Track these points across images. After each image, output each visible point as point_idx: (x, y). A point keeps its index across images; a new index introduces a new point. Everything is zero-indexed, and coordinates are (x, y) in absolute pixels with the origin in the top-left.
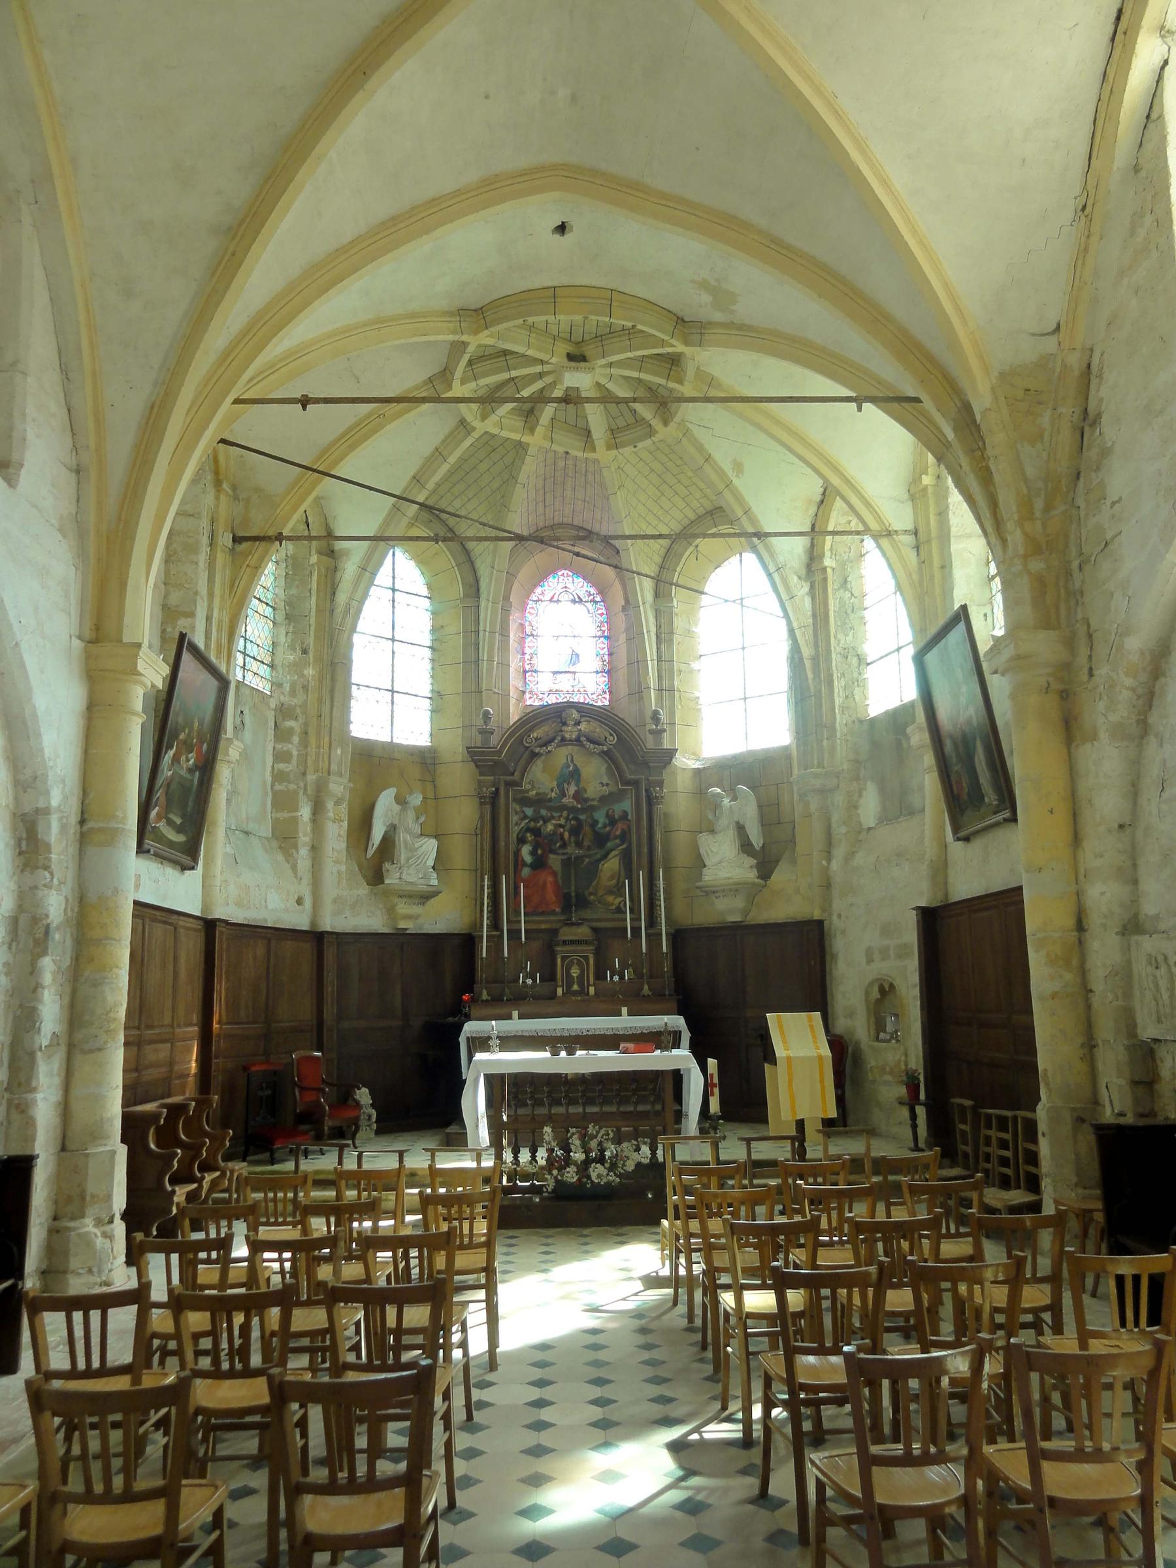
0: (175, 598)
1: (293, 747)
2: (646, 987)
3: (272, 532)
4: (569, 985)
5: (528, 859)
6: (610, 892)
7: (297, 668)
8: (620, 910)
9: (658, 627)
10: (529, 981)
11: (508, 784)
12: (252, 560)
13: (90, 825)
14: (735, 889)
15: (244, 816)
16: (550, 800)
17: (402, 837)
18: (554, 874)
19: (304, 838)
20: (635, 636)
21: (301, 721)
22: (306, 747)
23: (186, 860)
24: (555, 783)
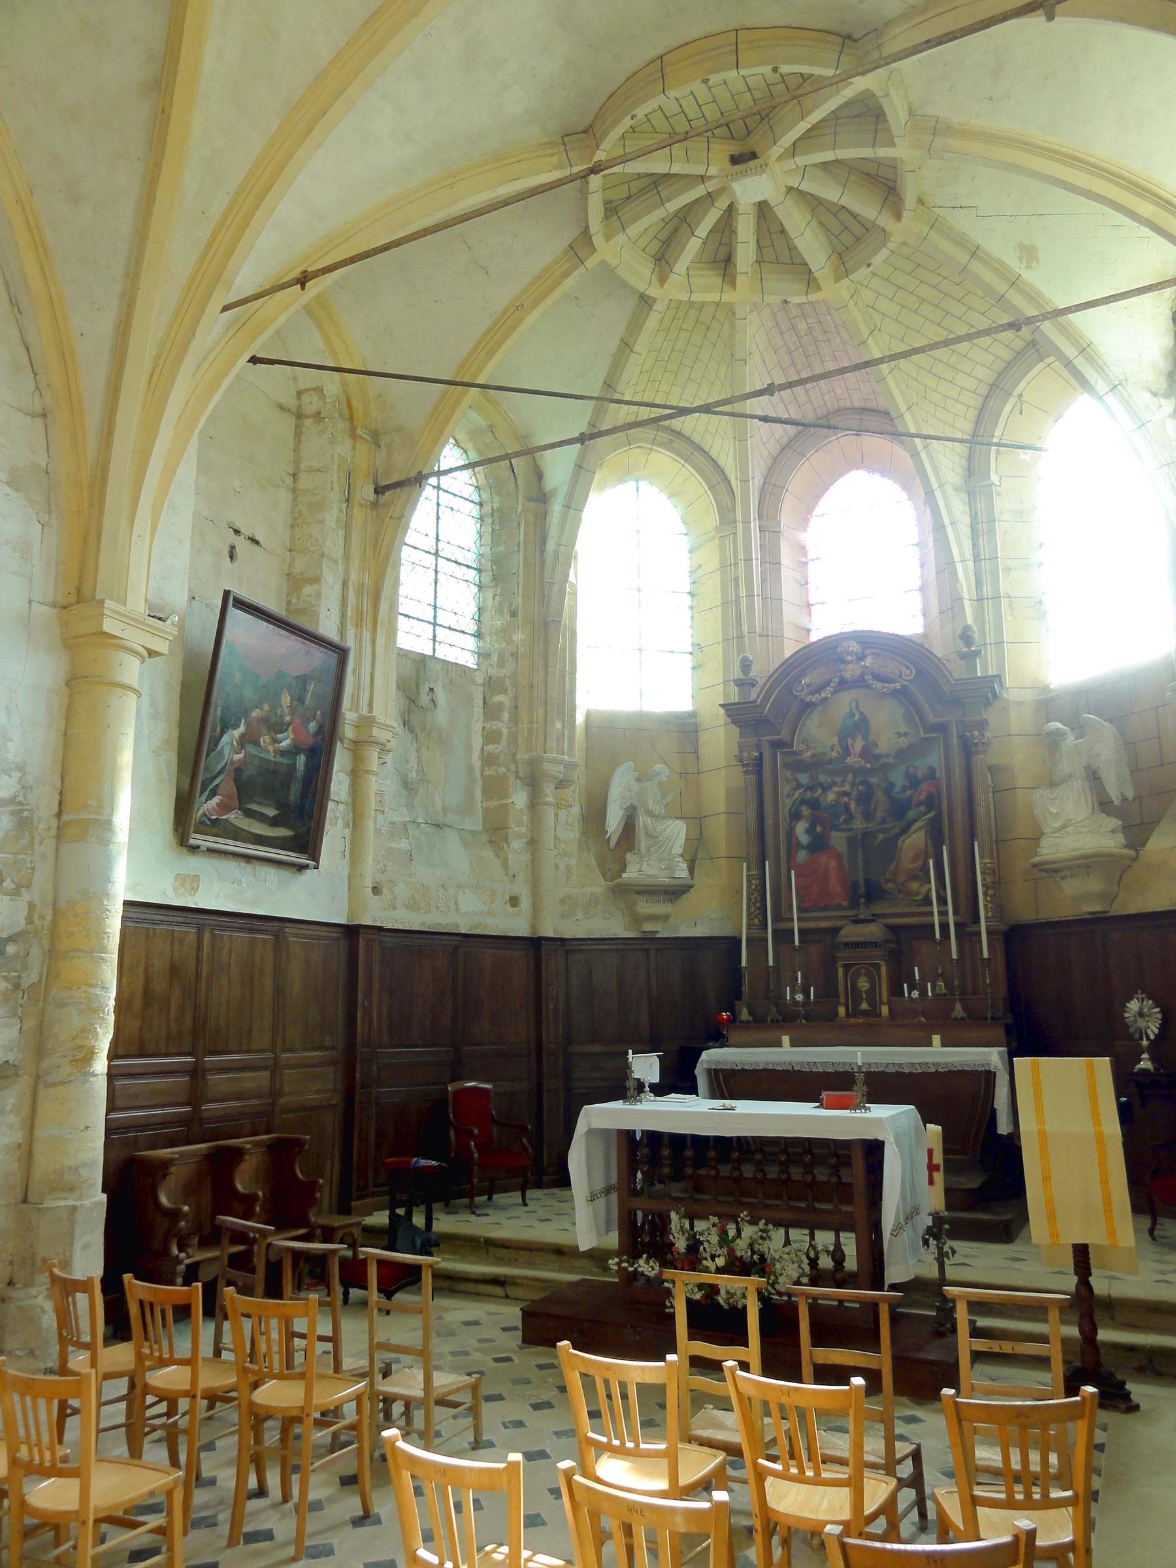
0: (299, 566)
1: (502, 726)
2: (958, 1006)
3: (413, 474)
4: (857, 1001)
5: (804, 839)
6: (915, 878)
7: (504, 633)
8: (927, 901)
9: (974, 516)
10: (799, 997)
11: (776, 745)
14: (1087, 864)
15: (439, 806)
16: (830, 761)
17: (642, 820)
18: (839, 857)
19: (518, 829)
21: (511, 693)
22: (516, 723)
24: (835, 740)
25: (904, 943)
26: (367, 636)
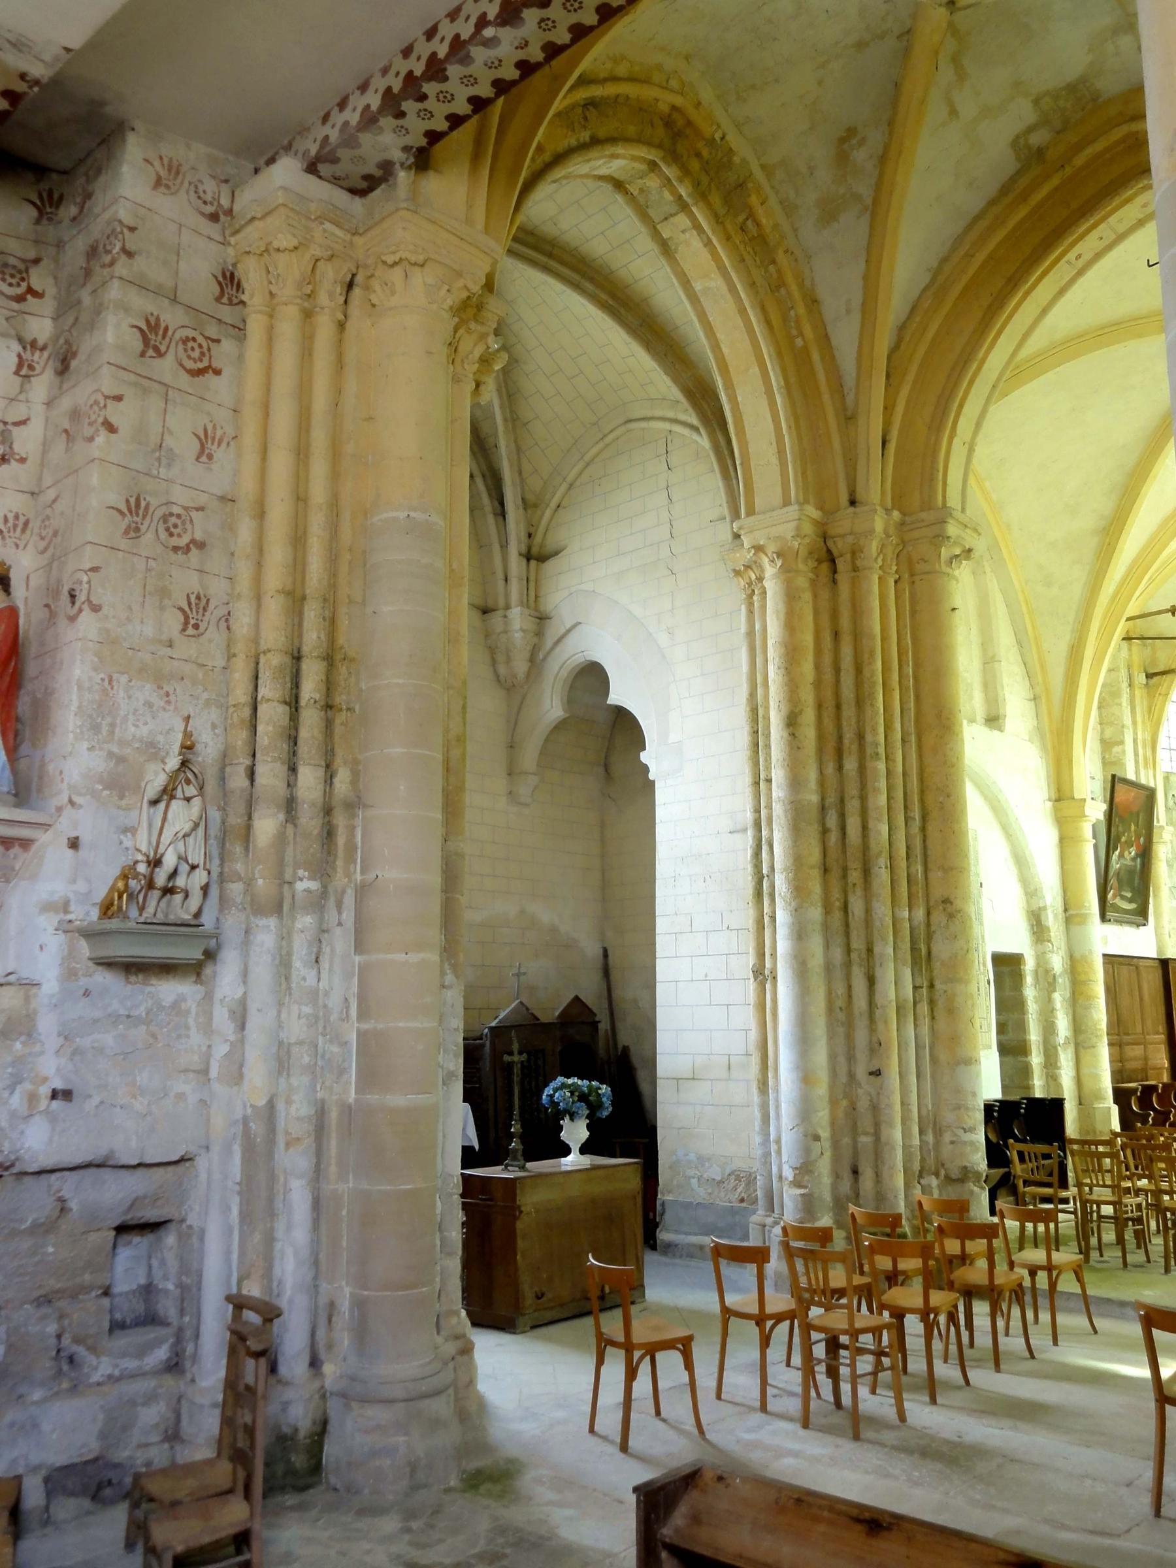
0: (1109, 732)
12: (1162, 690)
13: (1071, 912)
23: (1140, 919)
26: (1151, 772)
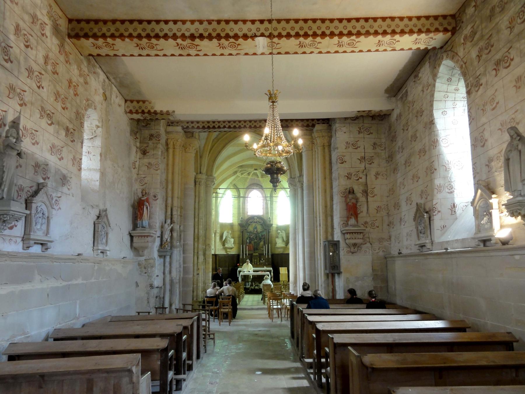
14: (281, 248)
17: (228, 239)
20: (267, 204)
25: (261, 255)
